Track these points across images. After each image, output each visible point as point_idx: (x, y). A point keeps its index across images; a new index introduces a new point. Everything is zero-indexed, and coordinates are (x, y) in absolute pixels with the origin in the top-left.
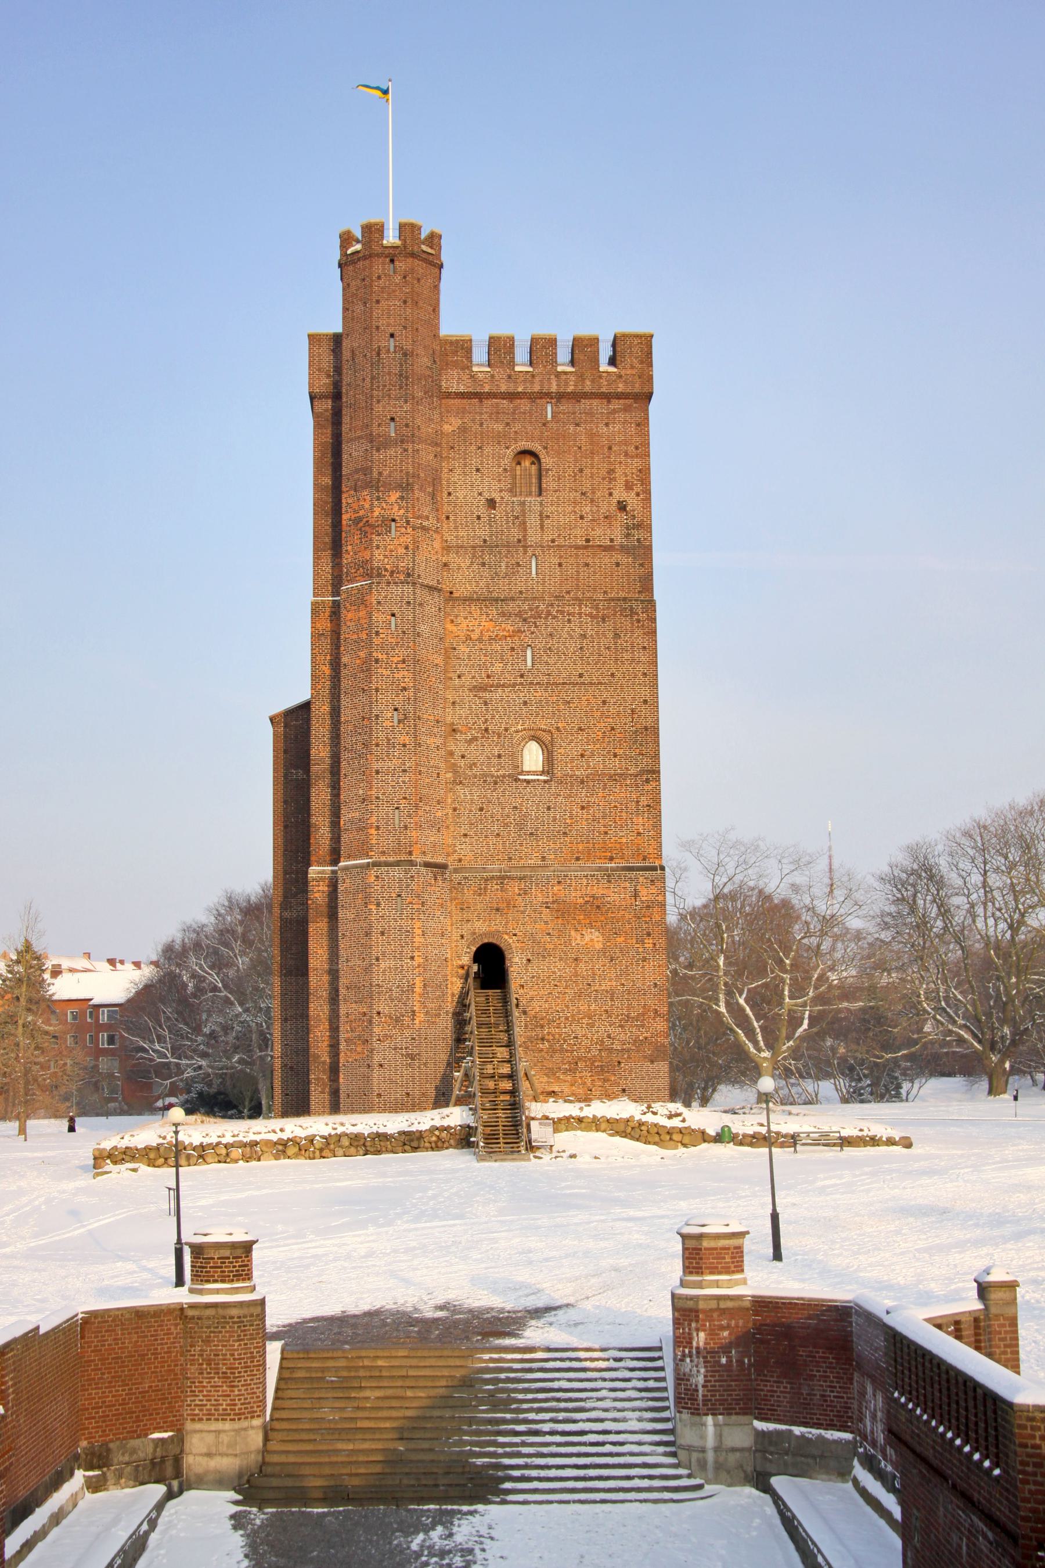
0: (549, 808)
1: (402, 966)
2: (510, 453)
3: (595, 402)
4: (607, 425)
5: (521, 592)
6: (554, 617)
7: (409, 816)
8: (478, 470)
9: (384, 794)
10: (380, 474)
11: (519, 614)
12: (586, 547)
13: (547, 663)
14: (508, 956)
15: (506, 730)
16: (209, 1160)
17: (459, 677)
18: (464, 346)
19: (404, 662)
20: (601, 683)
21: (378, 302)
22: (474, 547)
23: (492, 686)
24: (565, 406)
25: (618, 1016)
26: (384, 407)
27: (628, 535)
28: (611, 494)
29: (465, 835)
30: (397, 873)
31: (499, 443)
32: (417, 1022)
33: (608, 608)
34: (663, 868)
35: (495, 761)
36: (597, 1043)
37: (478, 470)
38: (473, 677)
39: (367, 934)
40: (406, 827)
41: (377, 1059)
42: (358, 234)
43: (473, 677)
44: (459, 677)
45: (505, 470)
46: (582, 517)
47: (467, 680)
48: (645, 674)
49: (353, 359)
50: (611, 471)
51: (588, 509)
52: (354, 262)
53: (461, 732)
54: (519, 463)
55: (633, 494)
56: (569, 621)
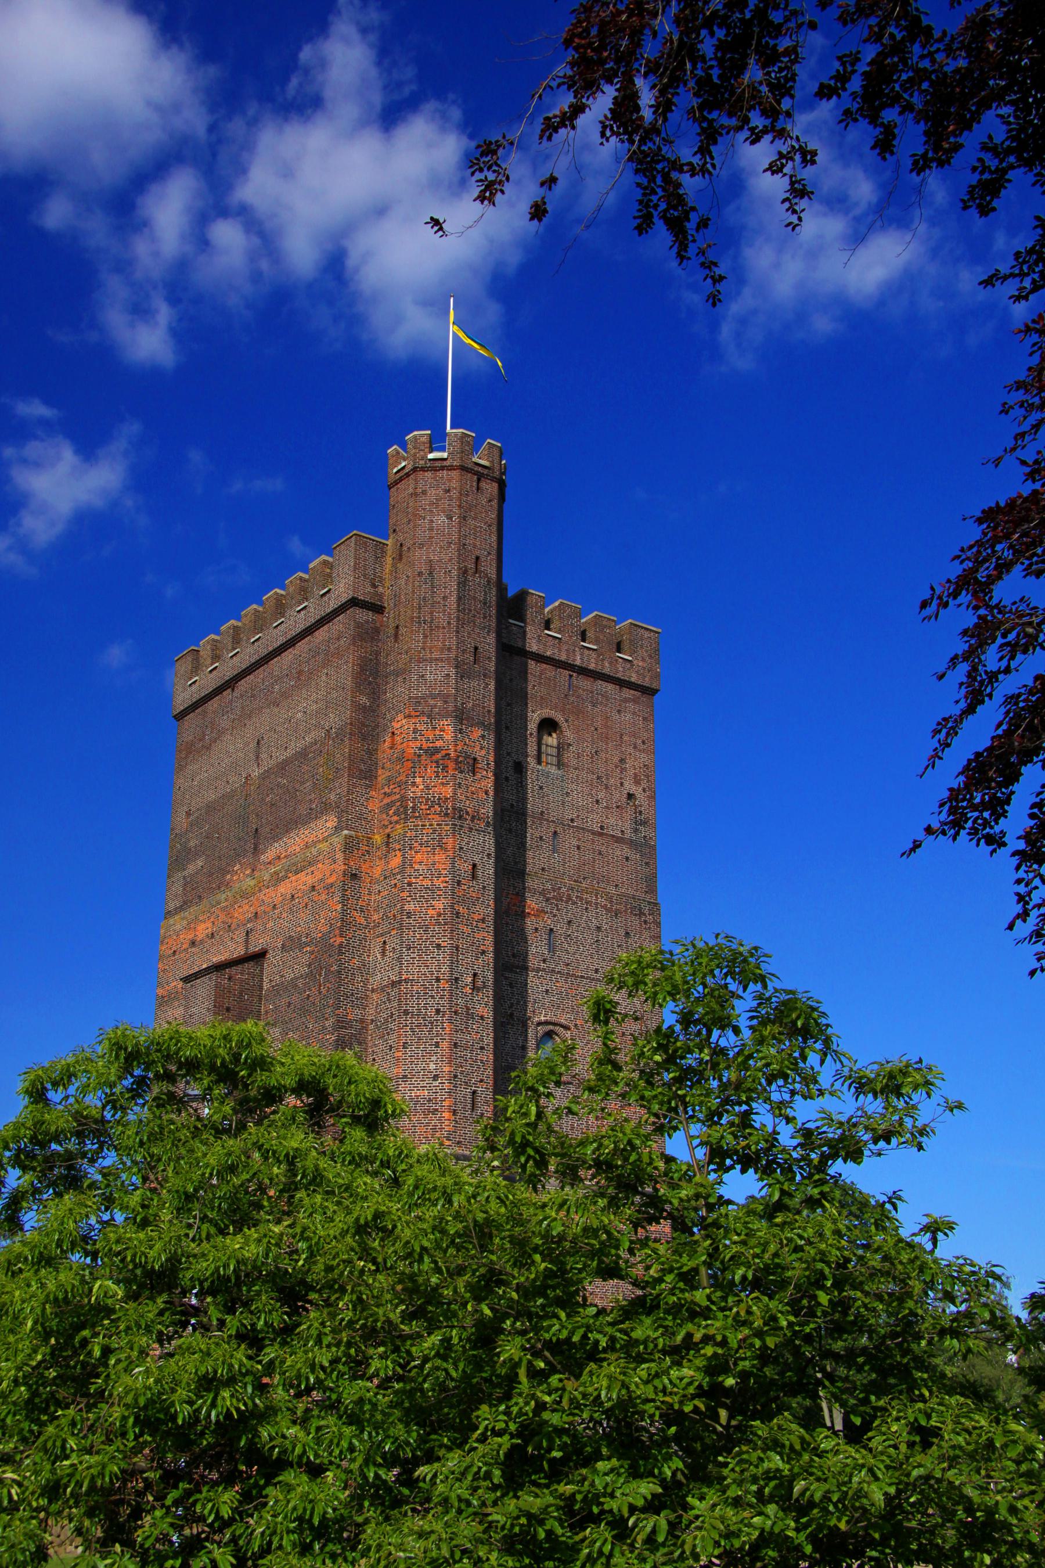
3: (610, 687)
4: (619, 711)
5: (543, 869)
6: (574, 903)
7: (487, 1102)
8: (507, 728)
9: (462, 1073)
11: (542, 893)
19: (483, 920)
21: (464, 518)
23: (518, 967)
24: (585, 683)
27: (636, 831)
49: (431, 573)
50: (622, 761)
52: (435, 469)
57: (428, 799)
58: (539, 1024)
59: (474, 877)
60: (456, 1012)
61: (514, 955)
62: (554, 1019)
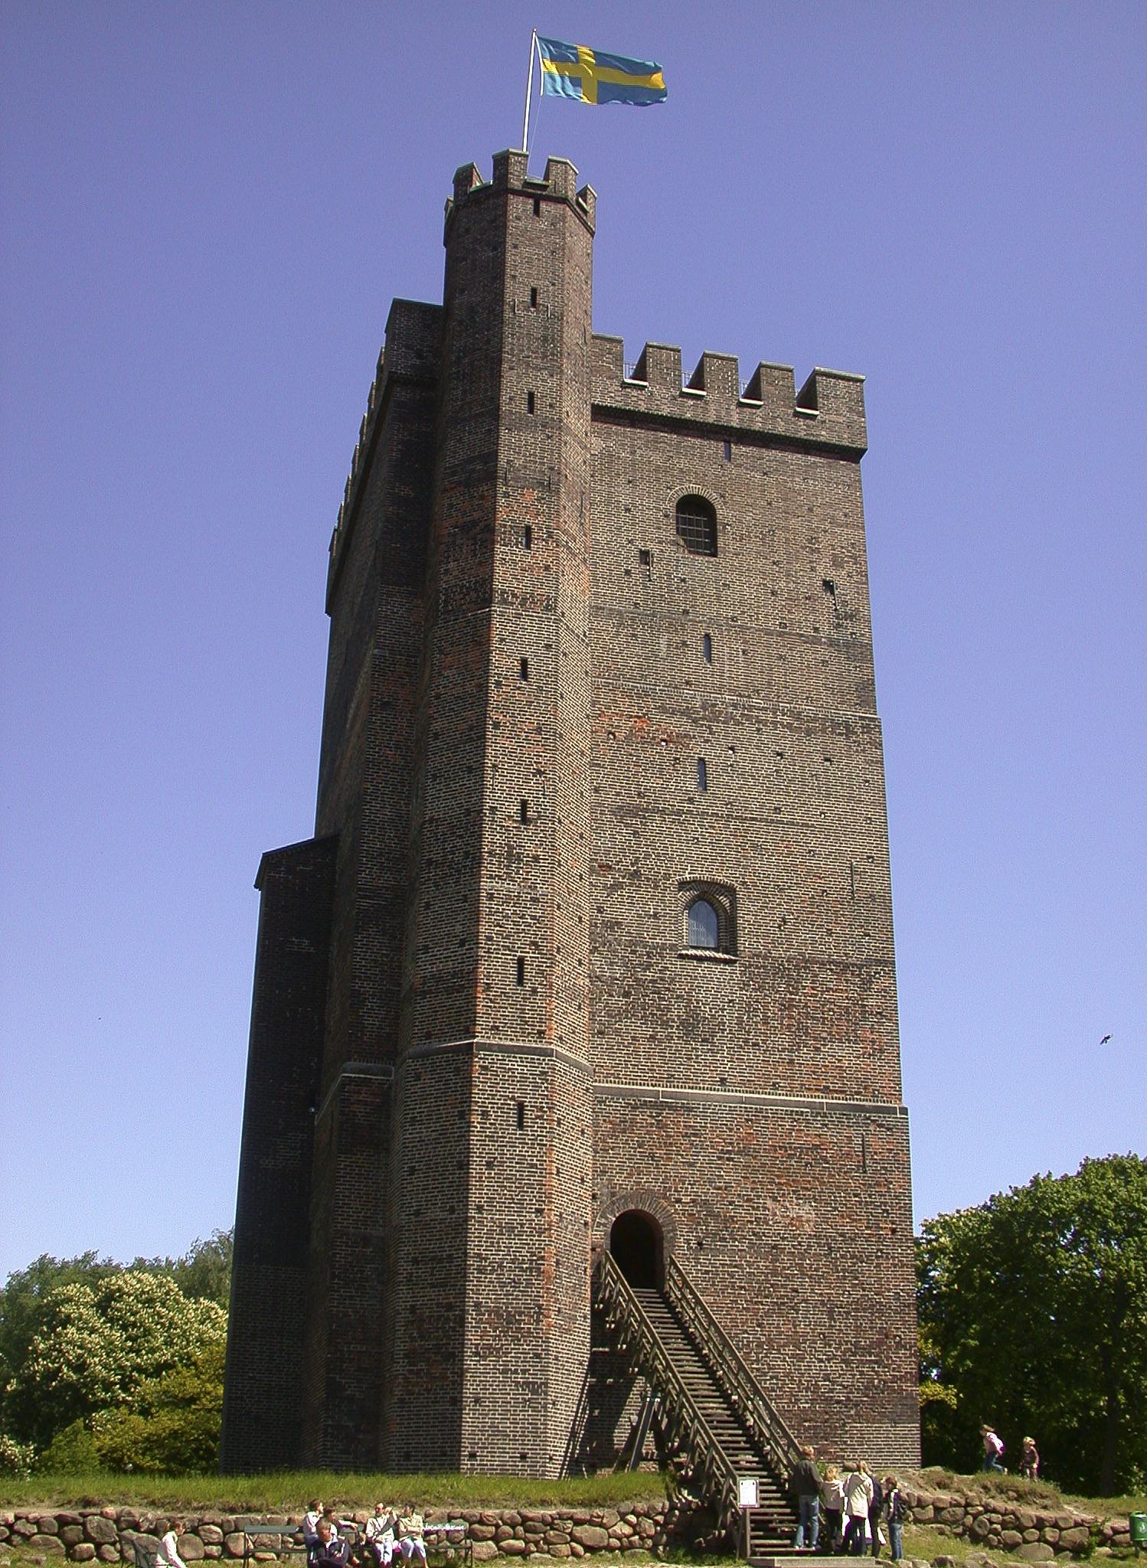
1: (522, 1225)
6: (738, 723)
12: (780, 634)
15: (667, 877)
20: (807, 825)
23: (646, 810)
25: (840, 1344)
26: (519, 376)
28: (813, 569)
31: (658, 480)
32: (543, 1325)
33: (815, 720)
34: (904, 1111)
36: (807, 1389)
37: (628, 510)
38: (618, 794)
40: (534, 991)
43: (618, 794)
46: (773, 593)
47: (609, 799)
51: (783, 584)
53: (599, 875)
57: (464, 586)
60: (491, 853)
62: (706, 877)
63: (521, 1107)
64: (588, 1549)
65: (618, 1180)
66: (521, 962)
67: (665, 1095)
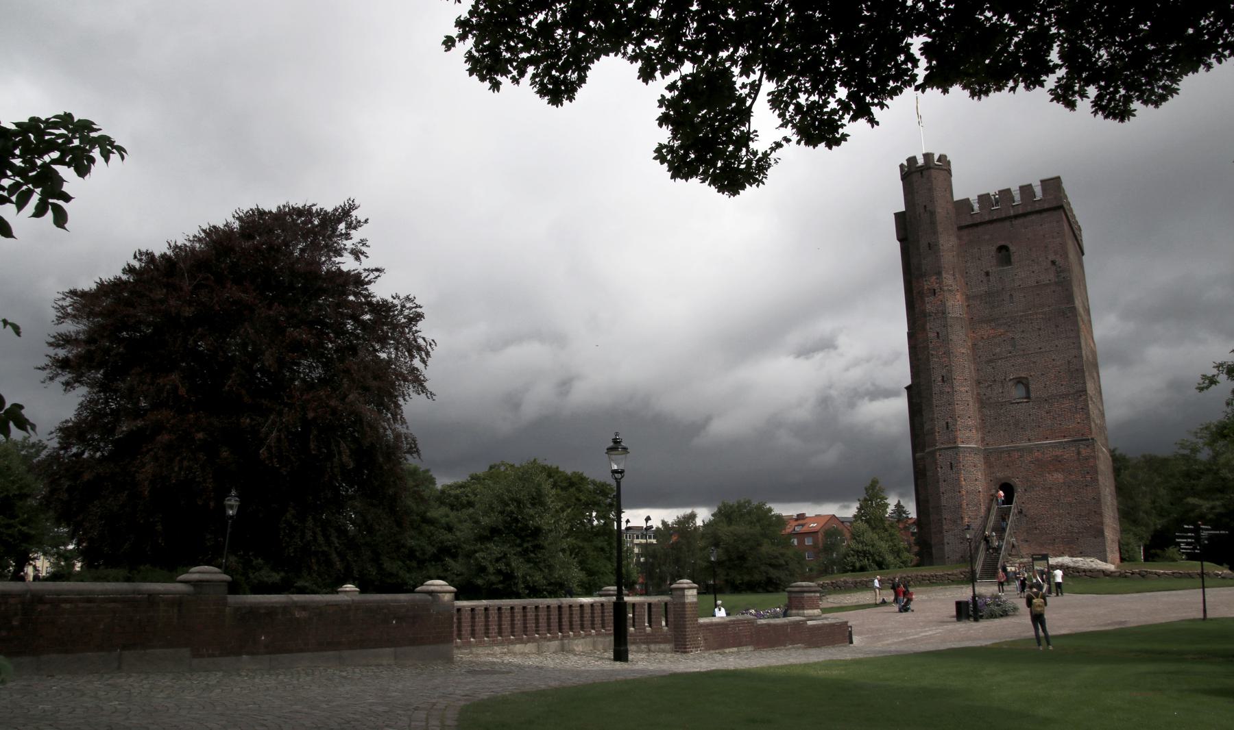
0: (1030, 415)
2: (994, 248)
3: (1033, 217)
10: (926, 270)
13: (1022, 345)
14: (1015, 488)
15: (1005, 379)
16: (859, 587)
17: (979, 357)
18: (966, 203)
21: (917, 192)
22: (981, 296)
24: (1017, 222)
27: (1058, 276)
29: (989, 432)
30: (950, 452)
35: (1001, 395)
37: (979, 259)
39: (938, 482)
40: (952, 430)
41: (946, 541)
42: (905, 163)
44: (979, 357)
45: (992, 257)
46: (1033, 272)
48: (1074, 343)
54: (1000, 252)
55: (1058, 256)
56: (1032, 323)
58: (1011, 380)
59: (938, 337)
61: (994, 355)
62: (1018, 376)
63: (951, 463)
64: (953, 581)
65: (998, 474)
66: (947, 423)
67: (1010, 447)
